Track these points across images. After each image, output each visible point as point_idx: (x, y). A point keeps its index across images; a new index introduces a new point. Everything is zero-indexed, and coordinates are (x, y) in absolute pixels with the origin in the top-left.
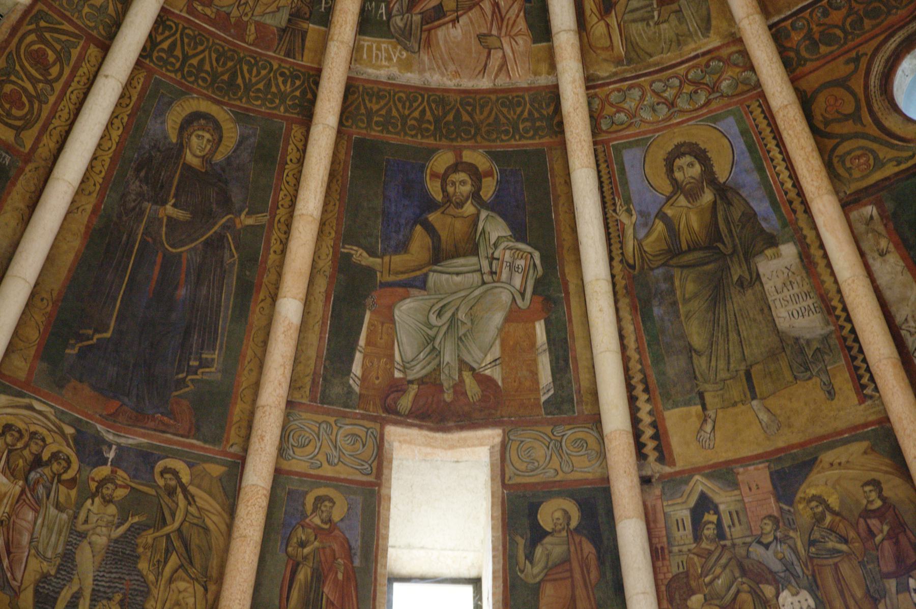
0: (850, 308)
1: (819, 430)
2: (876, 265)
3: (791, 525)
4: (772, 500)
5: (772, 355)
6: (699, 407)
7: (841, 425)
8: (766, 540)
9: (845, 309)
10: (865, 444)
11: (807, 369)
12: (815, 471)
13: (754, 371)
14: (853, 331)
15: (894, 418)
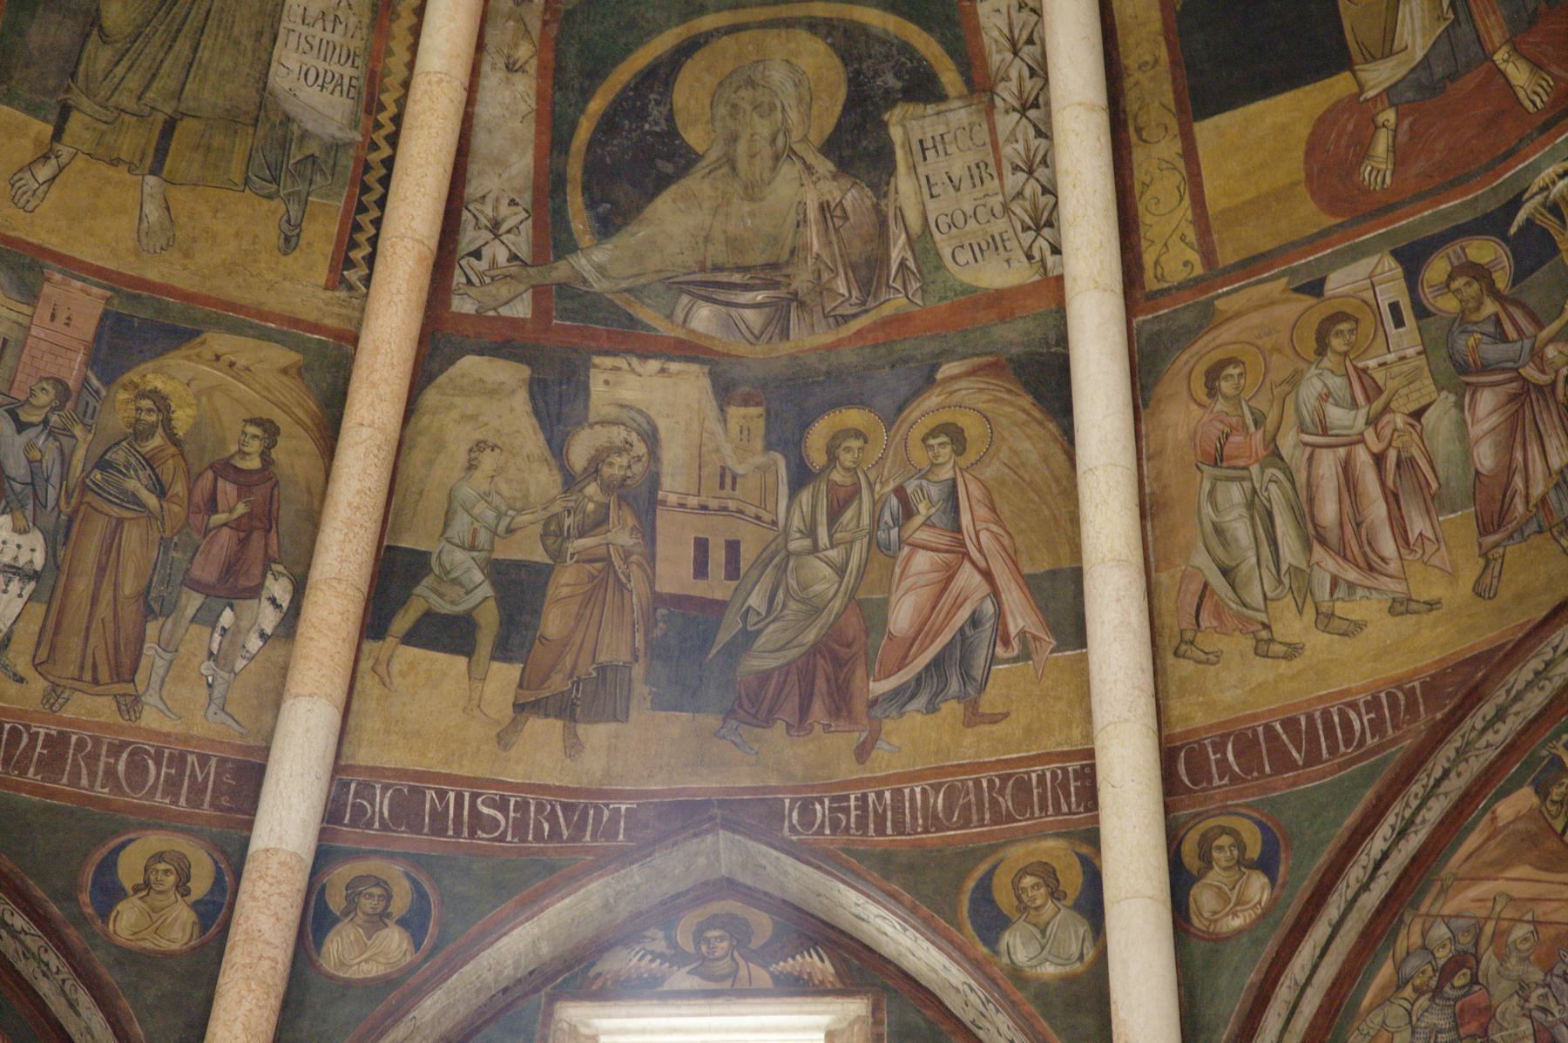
0: (408, 120)
1: (230, 289)
2: (492, 80)
3: (86, 416)
4: (80, 358)
5: (231, 120)
6: (50, 129)
7: (273, 302)
8: (24, 417)
9: (398, 120)
10: (291, 357)
11: (275, 180)
12: (184, 351)
13: (184, 125)
14: (389, 163)
15: (365, 342)
